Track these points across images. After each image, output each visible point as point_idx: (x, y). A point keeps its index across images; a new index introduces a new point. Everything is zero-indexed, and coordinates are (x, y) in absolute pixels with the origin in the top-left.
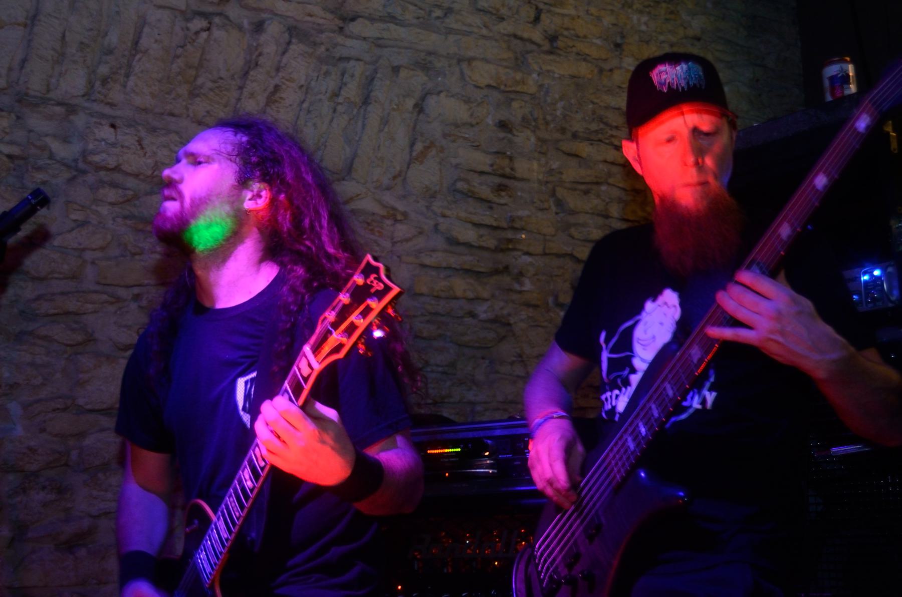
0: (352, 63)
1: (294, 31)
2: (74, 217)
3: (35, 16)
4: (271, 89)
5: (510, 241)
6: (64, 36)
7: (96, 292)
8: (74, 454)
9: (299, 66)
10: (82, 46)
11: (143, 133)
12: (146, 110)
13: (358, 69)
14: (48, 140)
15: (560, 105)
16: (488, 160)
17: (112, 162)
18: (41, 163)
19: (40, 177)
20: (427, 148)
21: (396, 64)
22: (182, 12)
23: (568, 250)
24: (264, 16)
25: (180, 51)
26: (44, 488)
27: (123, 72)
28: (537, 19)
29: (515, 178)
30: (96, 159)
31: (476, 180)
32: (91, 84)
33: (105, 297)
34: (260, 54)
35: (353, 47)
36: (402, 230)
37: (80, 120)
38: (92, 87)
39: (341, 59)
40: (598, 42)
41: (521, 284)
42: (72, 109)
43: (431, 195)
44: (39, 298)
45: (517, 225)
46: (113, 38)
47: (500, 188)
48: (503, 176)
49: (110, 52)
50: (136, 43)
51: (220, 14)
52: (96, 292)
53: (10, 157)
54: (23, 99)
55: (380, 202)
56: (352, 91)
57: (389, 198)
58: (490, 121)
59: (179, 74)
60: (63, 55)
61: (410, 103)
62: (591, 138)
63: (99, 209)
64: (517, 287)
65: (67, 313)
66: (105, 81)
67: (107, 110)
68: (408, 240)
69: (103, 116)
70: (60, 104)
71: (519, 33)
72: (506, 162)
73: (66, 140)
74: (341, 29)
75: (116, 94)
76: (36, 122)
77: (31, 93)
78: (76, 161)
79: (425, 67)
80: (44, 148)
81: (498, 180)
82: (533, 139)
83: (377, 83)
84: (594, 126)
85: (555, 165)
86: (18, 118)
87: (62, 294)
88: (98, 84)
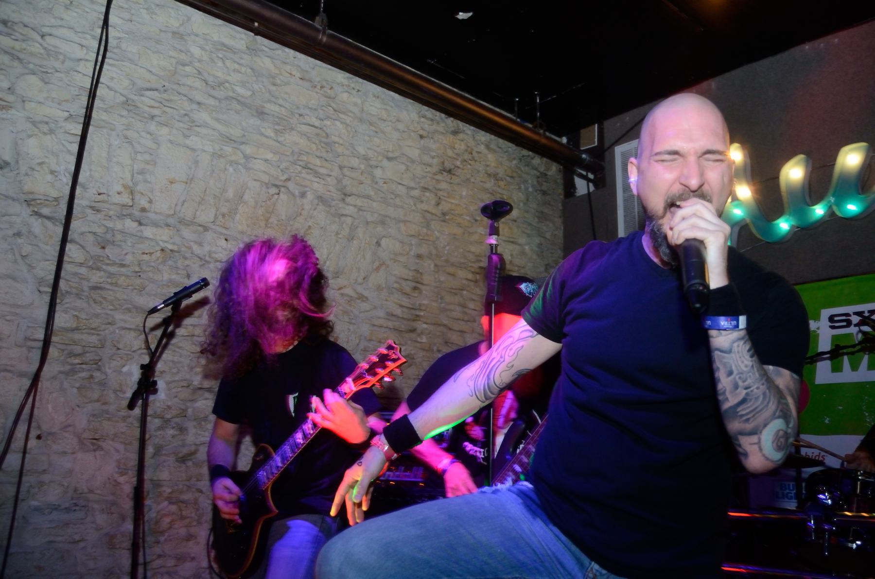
5: (417, 316)
8: (190, 410)
13: (349, 220)
14: (192, 244)
15: (447, 248)
16: (411, 274)
18: (187, 255)
19: (187, 262)
20: (381, 265)
22: (266, 184)
23: (445, 322)
26: (173, 428)
28: (438, 204)
29: (422, 284)
30: (217, 256)
31: (404, 283)
32: (216, 217)
36: (365, 306)
37: (209, 236)
39: (343, 215)
40: (468, 218)
41: (421, 338)
42: (206, 229)
43: (379, 288)
45: (423, 308)
47: (415, 288)
48: (417, 282)
49: (227, 201)
53: (171, 251)
54: (181, 221)
55: (355, 290)
56: (345, 232)
57: (360, 289)
58: (412, 253)
60: (203, 199)
62: (462, 266)
64: (419, 340)
65: (193, 336)
66: (224, 216)
67: (224, 231)
68: (367, 311)
69: (221, 234)
70: (200, 226)
71: (430, 210)
72: (419, 275)
73: (200, 244)
74: (344, 199)
76: (187, 233)
77: (187, 218)
78: (205, 256)
79: (383, 223)
80: (190, 248)
81: (414, 284)
82: (432, 266)
83: (359, 229)
84: (462, 261)
85: (442, 279)
88: (220, 217)
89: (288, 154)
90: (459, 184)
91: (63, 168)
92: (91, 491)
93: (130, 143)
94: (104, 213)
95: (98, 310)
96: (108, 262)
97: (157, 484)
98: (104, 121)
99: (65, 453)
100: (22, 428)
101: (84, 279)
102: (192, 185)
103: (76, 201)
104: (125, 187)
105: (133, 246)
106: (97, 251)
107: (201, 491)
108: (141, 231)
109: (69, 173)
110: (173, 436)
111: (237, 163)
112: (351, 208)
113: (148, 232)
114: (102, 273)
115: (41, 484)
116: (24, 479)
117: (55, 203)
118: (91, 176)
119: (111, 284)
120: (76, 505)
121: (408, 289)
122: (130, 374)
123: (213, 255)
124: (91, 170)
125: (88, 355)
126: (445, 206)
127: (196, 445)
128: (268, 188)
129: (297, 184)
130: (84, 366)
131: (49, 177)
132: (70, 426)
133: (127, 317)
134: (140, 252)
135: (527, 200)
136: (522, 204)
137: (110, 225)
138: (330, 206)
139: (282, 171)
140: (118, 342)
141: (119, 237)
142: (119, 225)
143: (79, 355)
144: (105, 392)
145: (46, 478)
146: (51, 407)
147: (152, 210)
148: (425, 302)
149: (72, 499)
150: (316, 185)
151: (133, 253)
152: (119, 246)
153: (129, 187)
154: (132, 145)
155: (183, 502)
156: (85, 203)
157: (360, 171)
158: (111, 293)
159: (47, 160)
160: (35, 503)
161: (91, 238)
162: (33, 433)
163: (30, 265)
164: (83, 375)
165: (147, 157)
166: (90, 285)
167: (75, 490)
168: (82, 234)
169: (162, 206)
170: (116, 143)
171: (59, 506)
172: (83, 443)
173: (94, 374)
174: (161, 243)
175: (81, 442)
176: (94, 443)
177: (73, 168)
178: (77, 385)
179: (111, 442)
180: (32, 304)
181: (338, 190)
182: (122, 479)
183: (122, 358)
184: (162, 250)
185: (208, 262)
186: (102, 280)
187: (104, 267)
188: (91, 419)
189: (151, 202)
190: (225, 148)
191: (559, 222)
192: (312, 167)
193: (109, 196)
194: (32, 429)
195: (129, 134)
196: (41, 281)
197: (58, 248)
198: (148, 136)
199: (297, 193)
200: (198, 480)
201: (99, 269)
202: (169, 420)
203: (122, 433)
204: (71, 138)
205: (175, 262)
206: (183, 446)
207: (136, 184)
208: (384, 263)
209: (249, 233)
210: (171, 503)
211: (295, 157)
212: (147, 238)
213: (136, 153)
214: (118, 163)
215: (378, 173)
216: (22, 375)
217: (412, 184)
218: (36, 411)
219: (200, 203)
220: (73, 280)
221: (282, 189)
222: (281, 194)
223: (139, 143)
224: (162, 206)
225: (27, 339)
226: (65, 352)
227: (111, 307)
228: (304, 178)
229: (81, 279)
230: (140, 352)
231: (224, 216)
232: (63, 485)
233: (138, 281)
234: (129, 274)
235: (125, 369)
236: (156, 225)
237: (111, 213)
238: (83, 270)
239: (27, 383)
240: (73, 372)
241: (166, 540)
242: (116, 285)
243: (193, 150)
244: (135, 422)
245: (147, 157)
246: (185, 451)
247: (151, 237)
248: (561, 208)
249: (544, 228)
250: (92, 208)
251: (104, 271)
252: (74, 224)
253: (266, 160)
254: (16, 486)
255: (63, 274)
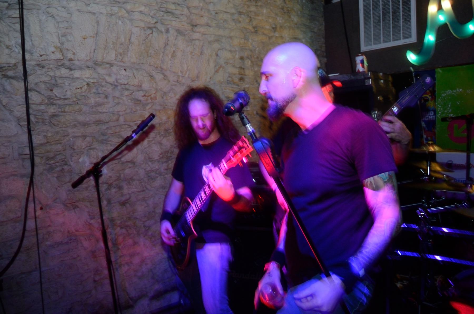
0: (197, 41)
1: (179, 32)
2: (115, 101)
3: (97, 33)
4: (172, 52)
6: (107, 40)
7: (124, 125)
8: (122, 175)
9: (181, 44)
10: (113, 43)
11: (135, 71)
12: (134, 63)
14: (105, 76)
16: (237, 70)
17: (126, 83)
18: (103, 84)
21: (209, 40)
24: (169, 26)
25: (144, 42)
26: (115, 187)
27: (126, 51)
28: (251, 20)
32: (116, 56)
33: (127, 126)
34: (168, 41)
35: (196, 36)
37: (114, 69)
38: (117, 56)
42: (111, 65)
44: (107, 128)
46: (122, 39)
48: (242, 74)
49: (122, 44)
50: (130, 40)
51: (155, 27)
52: (124, 125)
54: (96, 63)
58: (237, 56)
59: (144, 49)
61: (214, 54)
63: (123, 97)
65: (116, 133)
67: (122, 64)
69: (122, 66)
70: (108, 63)
73: (110, 75)
75: (126, 59)
76: (100, 70)
77: (98, 60)
78: (114, 82)
79: (217, 41)
80: (104, 79)
82: (250, 62)
85: (256, 69)
86: (94, 69)
87: (114, 126)
88: (119, 56)
89: (154, 4)
90: (261, 6)
91: (13, 42)
92: (77, 231)
93: (53, 17)
94: (47, 67)
95: (57, 129)
96: (56, 98)
97: (112, 220)
98: (32, 4)
99: (58, 214)
100: (31, 205)
101: (45, 112)
102: (98, 38)
103: (27, 63)
104: (56, 47)
105: (70, 85)
106: (50, 93)
107: (137, 218)
108: (72, 75)
109: (19, 46)
110: (115, 192)
111: (124, 18)
112: (198, 34)
113: (77, 74)
114: (54, 107)
115: (49, 233)
116: (39, 232)
117: (15, 67)
118: (33, 44)
119: (62, 112)
120: (70, 240)
121: (236, 80)
122: (84, 162)
123: (119, 81)
124: (32, 40)
125: (57, 157)
126: (255, 23)
127: (129, 194)
128: (145, 30)
129: (162, 24)
130: (57, 164)
131: (7, 51)
132: (57, 198)
133: (75, 130)
134: (74, 88)
135: (303, 9)
136: (299, 12)
137: (52, 74)
138: (185, 35)
139: (152, 17)
140: (73, 146)
141: (59, 81)
142: (58, 74)
143: (53, 158)
144: (72, 176)
145: (51, 229)
146: (43, 193)
147: (76, 59)
148: (247, 86)
149: (68, 237)
150: (174, 23)
151: (71, 90)
152: (61, 87)
153: (59, 47)
154: (54, 17)
155: (127, 226)
156: (33, 63)
157: (200, 8)
158: (62, 117)
159: (2, 40)
160: (48, 243)
161: (43, 86)
162: (38, 207)
163: (10, 110)
164: (58, 169)
165: (65, 24)
166: (50, 114)
167: (69, 232)
168: (36, 84)
169: (82, 55)
170: (43, 18)
171: (62, 242)
172: (66, 206)
173: (64, 167)
174: (86, 80)
175: (65, 205)
176: (72, 205)
177: (20, 41)
178: (56, 175)
179: (82, 203)
180: (17, 133)
181: (188, 23)
182: (92, 222)
183: (77, 154)
184: (88, 84)
185: (117, 86)
186: (56, 110)
187: (55, 102)
188: (68, 193)
189: (74, 54)
190: (114, 8)
191: (322, 20)
192: (170, 10)
193: (47, 55)
194: (36, 205)
195: (50, 10)
196: (19, 120)
197: (24, 96)
198: (63, 9)
199: (163, 30)
200: (134, 213)
201: (52, 104)
202: (111, 184)
203: (87, 196)
204: (14, 21)
205: (97, 89)
206: (122, 195)
207: (62, 44)
208: (221, 67)
209: (138, 63)
210: (121, 228)
211: (159, 6)
212: (77, 78)
213: (58, 23)
214: (48, 32)
215: (211, 7)
216: (22, 176)
217: (233, 11)
218: (36, 195)
219: (105, 49)
220: (38, 114)
221: (154, 29)
222: (154, 33)
223: (58, 16)
224: (82, 55)
225: (20, 155)
226: (44, 158)
227: (65, 126)
228: (166, 20)
229: (43, 112)
230: (87, 148)
231: (121, 55)
232: (61, 231)
233: (77, 107)
234: (70, 103)
235: (81, 160)
236: (80, 68)
237: (51, 66)
238: (43, 107)
239: (28, 181)
240: (51, 169)
241: (122, 247)
242: (64, 112)
243: (94, 14)
244: (93, 189)
245: (65, 24)
246: (124, 199)
247: (79, 77)
248: (323, 10)
249: (313, 26)
250: (38, 65)
251: (55, 104)
252: (31, 79)
253: (141, 12)
254: (36, 236)
255: (31, 111)
